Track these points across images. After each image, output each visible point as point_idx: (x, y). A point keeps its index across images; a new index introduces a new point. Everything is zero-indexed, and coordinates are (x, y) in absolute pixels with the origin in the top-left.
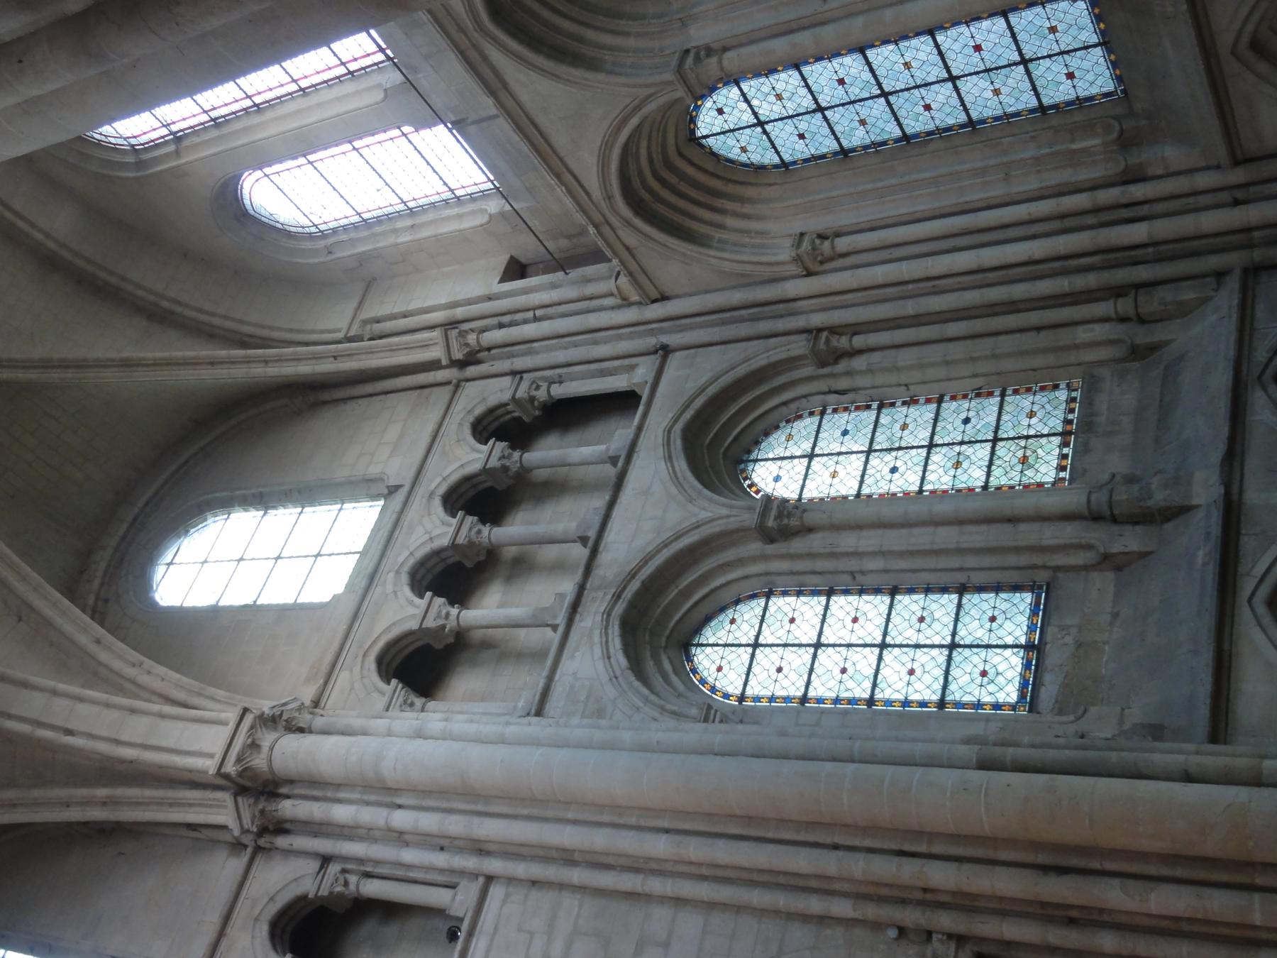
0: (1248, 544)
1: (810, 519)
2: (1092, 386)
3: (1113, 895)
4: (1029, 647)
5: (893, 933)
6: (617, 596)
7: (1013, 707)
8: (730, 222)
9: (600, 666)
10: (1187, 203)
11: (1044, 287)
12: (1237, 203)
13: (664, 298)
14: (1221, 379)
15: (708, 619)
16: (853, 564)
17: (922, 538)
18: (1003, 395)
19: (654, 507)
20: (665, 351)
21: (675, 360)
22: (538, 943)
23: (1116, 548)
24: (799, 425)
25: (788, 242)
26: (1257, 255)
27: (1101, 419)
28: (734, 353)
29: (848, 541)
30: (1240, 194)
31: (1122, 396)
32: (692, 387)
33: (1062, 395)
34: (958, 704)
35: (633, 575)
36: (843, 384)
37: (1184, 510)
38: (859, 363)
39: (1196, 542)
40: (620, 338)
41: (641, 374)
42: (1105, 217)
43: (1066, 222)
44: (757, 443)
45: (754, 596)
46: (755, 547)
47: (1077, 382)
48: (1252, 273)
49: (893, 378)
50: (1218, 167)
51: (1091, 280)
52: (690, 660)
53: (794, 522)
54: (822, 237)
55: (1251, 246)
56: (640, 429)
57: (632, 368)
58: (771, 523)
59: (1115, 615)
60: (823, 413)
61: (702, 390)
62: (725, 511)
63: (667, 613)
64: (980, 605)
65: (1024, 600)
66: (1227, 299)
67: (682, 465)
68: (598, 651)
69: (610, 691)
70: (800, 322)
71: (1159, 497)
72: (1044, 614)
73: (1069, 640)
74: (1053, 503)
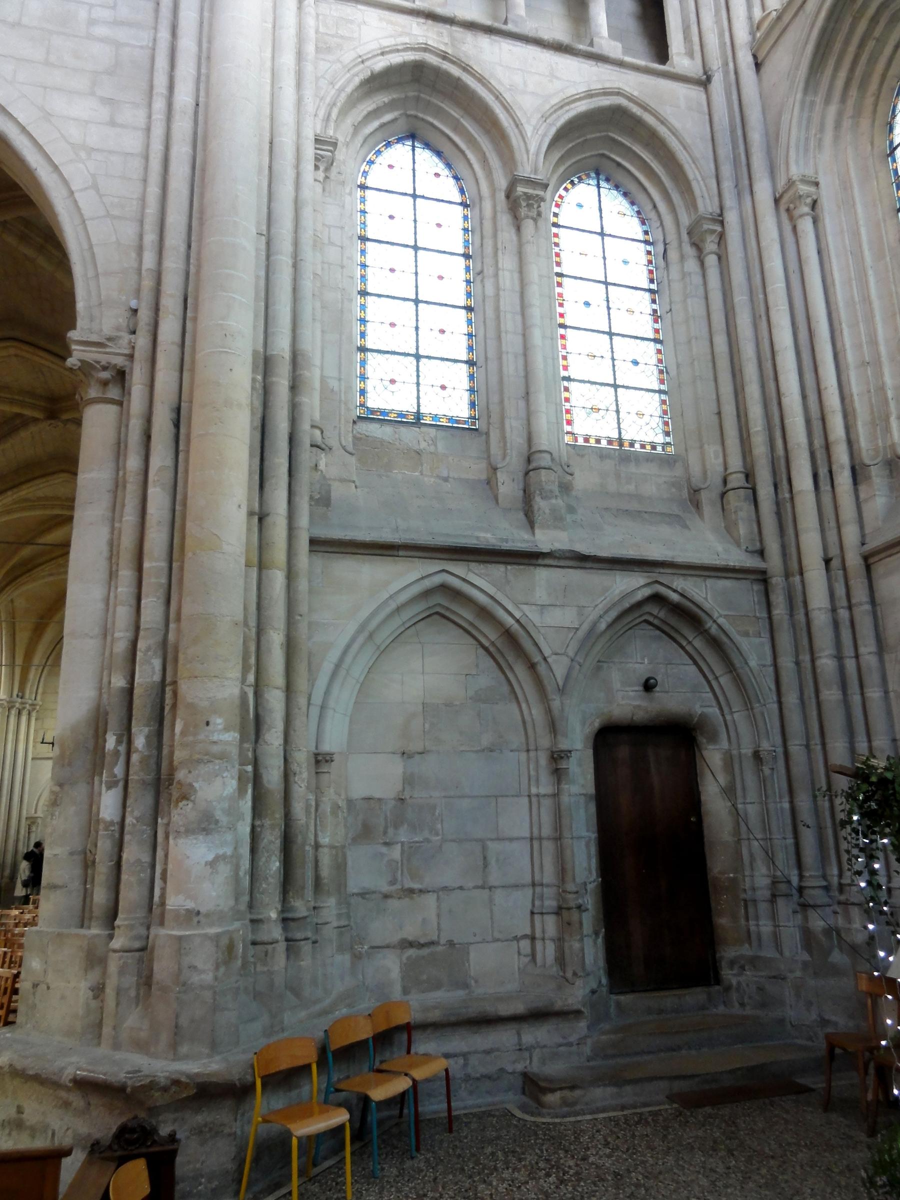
0: (498, 571)
1: (528, 226)
2: (666, 461)
3: (160, 458)
4: (418, 415)
5: (133, 304)
6: (445, 56)
7: (362, 405)
8: (833, 110)
9: (374, 46)
10: (831, 519)
11: (755, 412)
12: (827, 561)
13: (758, 66)
14: (655, 553)
15: (439, 154)
16: (489, 271)
17: (511, 323)
18: (660, 392)
19: (535, 85)
20: (705, 82)
21: (696, 93)
22: (106, 14)
23: (501, 476)
24: (636, 221)
25: (809, 172)
26: (777, 581)
27: (632, 468)
28: (702, 149)
29: (507, 262)
30: (835, 563)
31: (654, 485)
32: (667, 112)
33: (660, 439)
34: (363, 363)
35: (466, 69)
36: (673, 255)
37: (531, 523)
38: (692, 265)
39: (508, 533)
40: (721, 35)
41: (681, 59)
42: (820, 455)
43: (817, 422)
44: (617, 187)
45: (462, 191)
46: (502, 183)
47: (671, 450)
48: (762, 578)
49: (677, 298)
50: (863, 544)
51: (760, 447)
52: (399, 140)
53: (523, 211)
54: (814, 204)
55: (787, 575)
56: (621, 64)
57: (690, 54)
58: (520, 189)
59: (446, 480)
60: (646, 242)
61: (663, 122)
62: (533, 149)
63: (439, 113)
64: (460, 376)
65: (463, 412)
66: (737, 558)
67: (582, 107)
68: (387, 43)
69: (348, 57)
70: (730, 201)
71: (541, 504)
72: (452, 429)
73: (423, 445)
74: (542, 423)
